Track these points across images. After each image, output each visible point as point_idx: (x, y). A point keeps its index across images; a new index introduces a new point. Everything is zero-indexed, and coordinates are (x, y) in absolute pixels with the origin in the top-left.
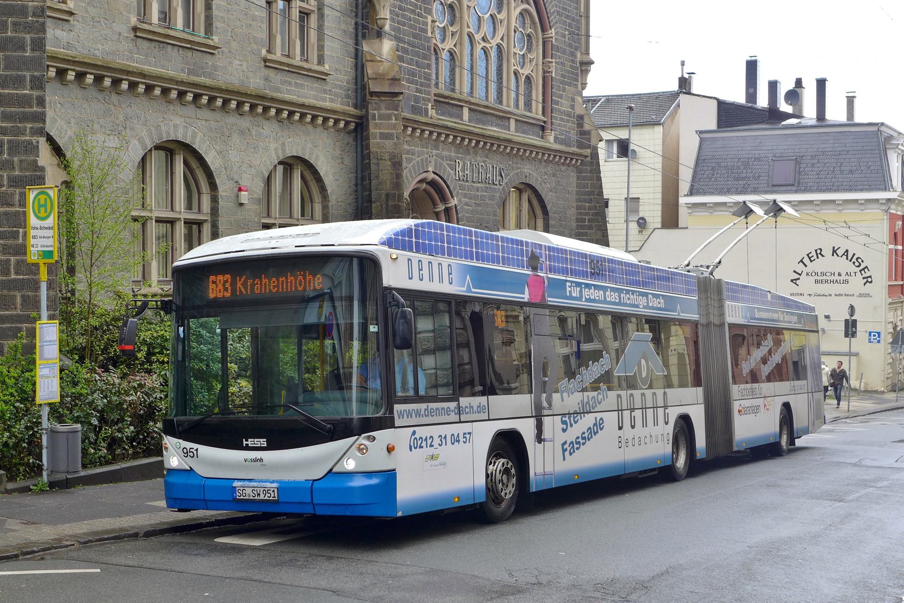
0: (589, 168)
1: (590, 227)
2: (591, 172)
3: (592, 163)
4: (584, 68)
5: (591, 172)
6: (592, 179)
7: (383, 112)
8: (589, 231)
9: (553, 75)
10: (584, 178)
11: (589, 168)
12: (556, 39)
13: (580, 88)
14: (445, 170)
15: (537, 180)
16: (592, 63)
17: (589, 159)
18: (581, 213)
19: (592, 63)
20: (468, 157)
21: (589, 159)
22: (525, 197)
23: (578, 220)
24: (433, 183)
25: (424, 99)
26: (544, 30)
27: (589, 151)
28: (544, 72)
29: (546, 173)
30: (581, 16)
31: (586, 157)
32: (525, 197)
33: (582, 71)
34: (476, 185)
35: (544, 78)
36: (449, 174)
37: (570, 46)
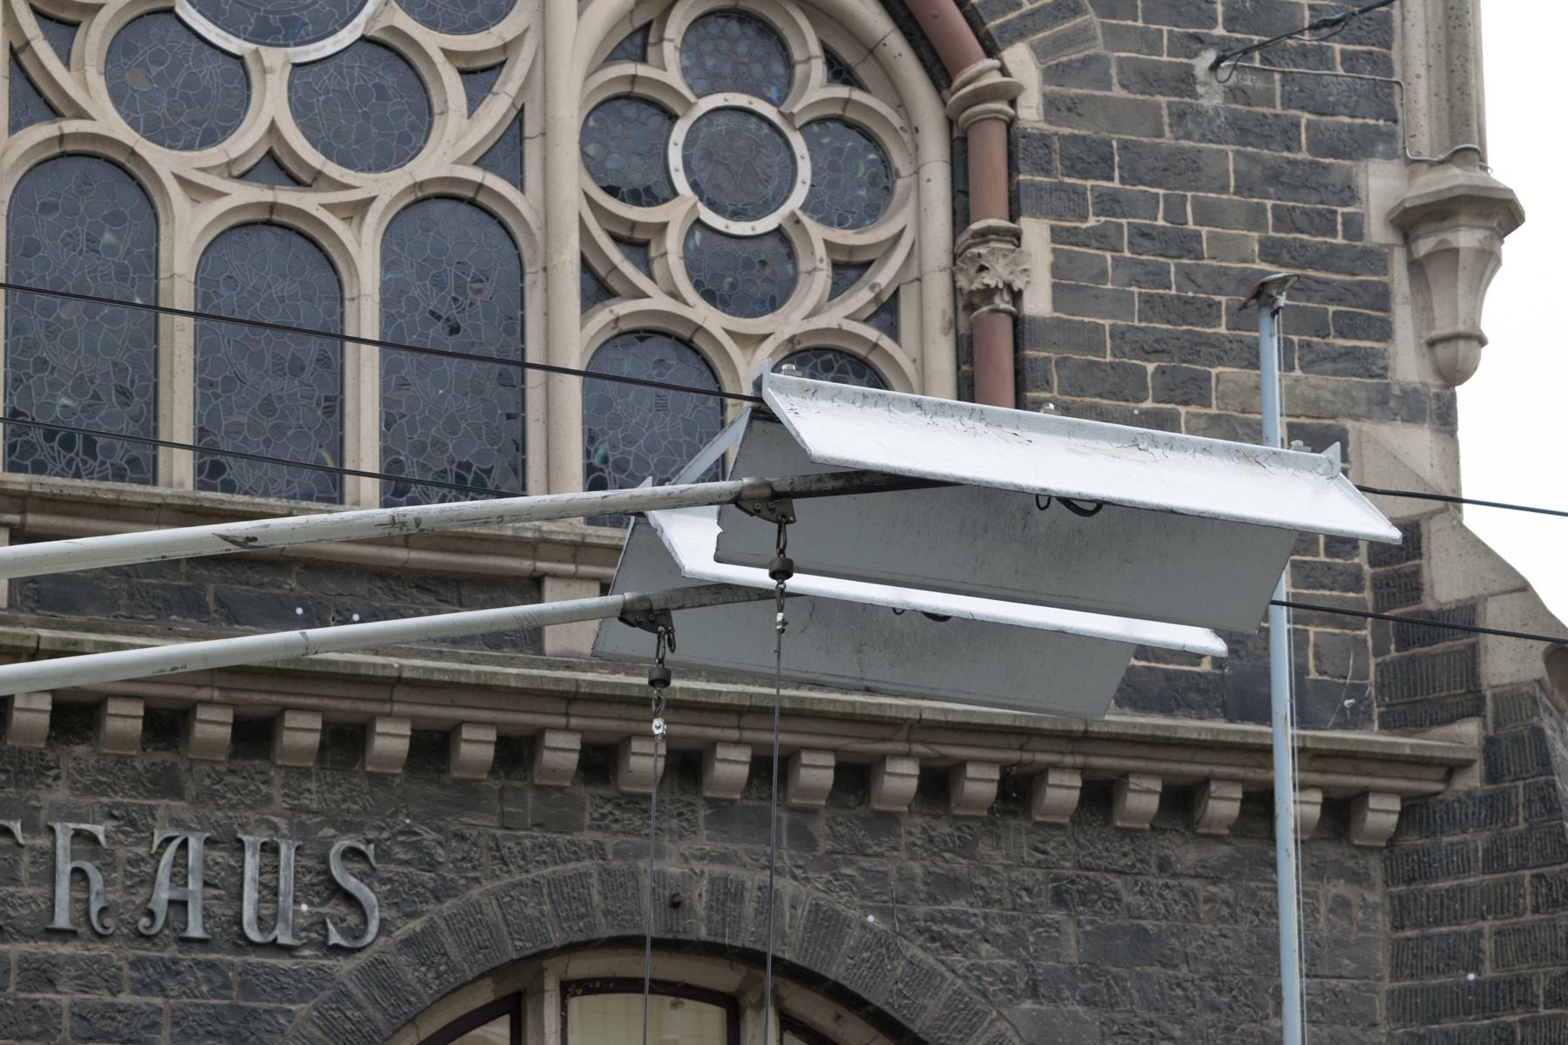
0: (1478, 840)
2: (1495, 858)
3: (1494, 807)
4: (1424, 246)
6: (1502, 904)
9: (1038, 303)
11: (1478, 840)
12: (1052, 105)
13: (1408, 364)
17: (1472, 781)
21: (1472, 781)
26: (940, 72)
27: (1470, 730)
28: (967, 302)
29: (953, 885)
31: (1452, 769)
33: (1416, 267)
37: (1242, 130)
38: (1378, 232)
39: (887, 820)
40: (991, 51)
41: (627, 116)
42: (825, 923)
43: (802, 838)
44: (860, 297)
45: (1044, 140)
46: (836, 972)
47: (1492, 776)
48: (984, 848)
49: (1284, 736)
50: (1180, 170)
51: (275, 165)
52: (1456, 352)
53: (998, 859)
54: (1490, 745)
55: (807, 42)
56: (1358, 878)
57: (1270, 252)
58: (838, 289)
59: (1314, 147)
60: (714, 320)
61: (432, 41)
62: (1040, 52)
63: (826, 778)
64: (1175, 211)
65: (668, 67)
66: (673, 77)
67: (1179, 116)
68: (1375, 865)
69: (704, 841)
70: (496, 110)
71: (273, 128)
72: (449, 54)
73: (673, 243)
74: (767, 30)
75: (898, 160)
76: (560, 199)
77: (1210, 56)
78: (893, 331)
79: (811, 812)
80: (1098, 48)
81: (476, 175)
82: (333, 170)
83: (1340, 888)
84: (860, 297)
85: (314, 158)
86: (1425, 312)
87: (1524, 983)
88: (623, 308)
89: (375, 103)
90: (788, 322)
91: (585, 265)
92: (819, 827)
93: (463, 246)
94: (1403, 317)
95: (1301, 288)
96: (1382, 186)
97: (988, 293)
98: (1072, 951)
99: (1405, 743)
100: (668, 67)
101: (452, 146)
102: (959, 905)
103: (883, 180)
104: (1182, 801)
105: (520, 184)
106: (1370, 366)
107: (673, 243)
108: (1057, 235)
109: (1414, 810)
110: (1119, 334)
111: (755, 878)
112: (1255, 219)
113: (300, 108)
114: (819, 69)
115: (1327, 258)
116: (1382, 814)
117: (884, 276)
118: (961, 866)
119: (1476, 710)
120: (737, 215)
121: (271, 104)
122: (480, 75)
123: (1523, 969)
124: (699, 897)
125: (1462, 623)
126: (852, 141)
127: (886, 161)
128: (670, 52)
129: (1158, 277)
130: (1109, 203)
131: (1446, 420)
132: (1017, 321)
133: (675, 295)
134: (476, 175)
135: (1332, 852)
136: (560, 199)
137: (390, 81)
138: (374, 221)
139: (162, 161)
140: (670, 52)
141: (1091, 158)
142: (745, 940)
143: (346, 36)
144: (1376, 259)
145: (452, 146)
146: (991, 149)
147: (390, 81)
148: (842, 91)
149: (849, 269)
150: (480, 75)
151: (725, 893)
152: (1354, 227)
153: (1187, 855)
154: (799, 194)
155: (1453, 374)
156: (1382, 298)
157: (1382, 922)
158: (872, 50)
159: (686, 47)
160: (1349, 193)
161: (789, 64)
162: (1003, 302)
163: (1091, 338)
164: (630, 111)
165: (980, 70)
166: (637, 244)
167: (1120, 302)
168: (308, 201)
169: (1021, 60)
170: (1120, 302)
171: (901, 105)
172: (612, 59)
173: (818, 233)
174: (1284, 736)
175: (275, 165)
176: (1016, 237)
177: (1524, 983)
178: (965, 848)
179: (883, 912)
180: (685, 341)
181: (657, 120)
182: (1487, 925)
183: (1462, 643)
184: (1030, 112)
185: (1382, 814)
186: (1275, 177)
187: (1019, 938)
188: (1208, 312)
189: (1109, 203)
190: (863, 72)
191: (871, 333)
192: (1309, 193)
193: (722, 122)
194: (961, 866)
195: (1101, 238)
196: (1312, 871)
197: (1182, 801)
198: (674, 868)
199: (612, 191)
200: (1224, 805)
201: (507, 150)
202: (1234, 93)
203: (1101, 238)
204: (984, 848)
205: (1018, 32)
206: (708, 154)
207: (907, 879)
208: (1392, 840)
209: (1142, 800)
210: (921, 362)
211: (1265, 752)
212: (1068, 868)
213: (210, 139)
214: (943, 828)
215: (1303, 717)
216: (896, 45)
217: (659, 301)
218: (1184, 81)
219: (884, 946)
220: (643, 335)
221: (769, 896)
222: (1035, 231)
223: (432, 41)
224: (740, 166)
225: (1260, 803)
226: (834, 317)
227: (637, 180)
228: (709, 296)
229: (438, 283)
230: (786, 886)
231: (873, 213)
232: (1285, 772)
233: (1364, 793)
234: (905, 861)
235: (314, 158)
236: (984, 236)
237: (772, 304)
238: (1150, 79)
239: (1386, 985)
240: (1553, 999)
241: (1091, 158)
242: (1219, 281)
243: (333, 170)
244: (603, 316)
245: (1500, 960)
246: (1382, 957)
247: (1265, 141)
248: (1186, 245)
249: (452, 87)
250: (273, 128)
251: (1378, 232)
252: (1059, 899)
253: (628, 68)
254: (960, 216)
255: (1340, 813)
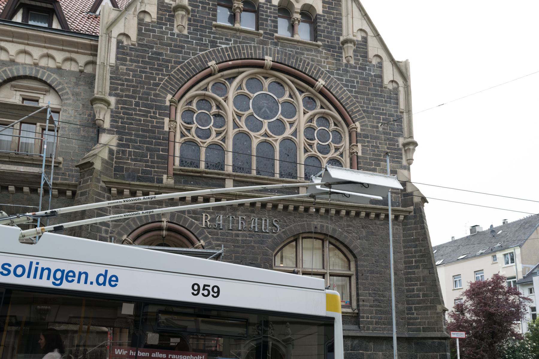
0: (413, 221)
1: (417, 267)
2: (415, 223)
3: (415, 217)
4: (406, 148)
5: (415, 223)
6: (416, 229)
7: (86, 178)
8: (416, 270)
9: (360, 154)
10: (410, 229)
11: (413, 221)
12: (361, 130)
13: (404, 163)
14: (186, 220)
15: (334, 230)
16: (415, 144)
17: (412, 214)
18: (408, 257)
19: (415, 144)
20: (222, 212)
21: (412, 214)
22: (327, 243)
23: (405, 262)
24: (169, 229)
25: (155, 172)
26: (348, 125)
27: (412, 208)
28: (351, 153)
29: (350, 226)
30: (402, 112)
31: (410, 212)
32: (327, 243)
33: (405, 151)
34: (234, 232)
35: (351, 160)
36: (192, 224)
37: (384, 133)
38: (401, 146)
39: (342, 217)
40: (354, 123)
41: (309, 130)
42: (334, 230)
43: (331, 220)
44: (338, 153)
45: (360, 134)
46: (335, 236)
47: (415, 213)
48: (354, 221)
49: (390, 208)
50: (377, 138)
51: (266, 135)
52: (410, 161)
53: (355, 223)
54: (414, 209)
55: (331, 121)
56: (399, 225)
57: (388, 148)
58: (335, 152)
59: (393, 135)
60: (320, 155)
61: (285, 120)
62: (360, 123)
63: (334, 212)
64: (376, 143)
65: (314, 124)
66: (315, 125)
67: (377, 131)
68: (401, 224)
69: (319, 220)
70: (293, 128)
71: (266, 130)
72: (288, 121)
73: (315, 145)
74: (327, 119)
75: (343, 136)
76: (301, 140)
77: (380, 124)
78: (342, 157)
79: (332, 216)
80: (367, 123)
81: (291, 136)
82: (273, 135)
83: (397, 227)
84: (338, 153)
85: (271, 134)
86: (406, 156)
87: (419, 238)
88: (309, 153)
89: (278, 127)
90: (329, 156)
91: (304, 148)
92: (333, 218)
93: (289, 145)
94: (404, 157)
95: (391, 153)
96: (401, 141)
97: (354, 153)
98: (364, 234)
99: (404, 209)
100: (314, 124)
101: (288, 133)
102: (350, 228)
103: (341, 138)
104: (377, 216)
105: (296, 138)
106: (400, 163)
107: (315, 145)
108: (362, 146)
109: (405, 217)
110: (369, 158)
111: (325, 225)
112: (386, 144)
113: (269, 128)
114: (333, 124)
115: (394, 149)
116: (402, 218)
117: (341, 150)
118: (351, 223)
119: (413, 205)
120: (323, 142)
121: (265, 127)
122: (291, 124)
123: (418, 237)
124: (319, 227)
125: (411, 194)
126: (337, 133)
127: (341, 136)
128: (315, 122)
129: (374, 151)
130: (368, 142)
131: (409, 169)
132: (357, 156)
133: (315, 152)
134: (291, 136)
135: (396, 222)
136: (301, 140)
137: (280, 124)
138: (278, 142)
139: (252, 134)
140: (315, 122)
141: (366, 136)
142: (324, 232)
143: (275, 119)
144: (400, 150)
145: (288, 133)
146: (354, 135)
147: (280, 124)
148: (336, 127)
149: (337, 149)
150: (291, 124)
151: (322, 226)
152: (398, 145)
153: (378, 222)
154: (331, 140)
155: (410, 164)
156: (401, 154)
157: (402, 231)
158: (339, 122)
159: (317, 121)
160: (397, 141)
161: (329, 124)
162: (355, 154)
163: (366, 159)
164: (310, 129)
165: (353, 125)
166: (311, 145)
167: (370, 154)
168: (270, 139)
169: (358, 124)
170: (370, 154)
171: (343, 129)
172: (308, 122)
173: (333, 145)
174: (390, 208)
175: (266, 135)
176: (357, 146)
177: (419, 238)
178: (351, 221)
179: (341, 229)
180: (317, 158)
181: (313, 130)
182: (414, 231)
183: (411, 197)
184: (359, 130)
185: (402, 218)
186: (388, 139)
187: (358, 232)
188: (380, 156)
189: (368, 142)
190: (338, 125)
191: (339, 157)
192: (393, 141)
193: (321, 131)
194: (351, 223)
195: (368, 146)
196: (393, 225)
197: (377, 216)
198: (315, 223)
199: (308, 139)
200: (383, 216)
201: (295, 133)
202: (383, 129)
203: (368, 146)
204: (354, 221)
205: (357, 120)
206: (320, 135)
207: (344, 225)
208: (403, 221)
209: (373, 215)
210: (346, 161)
211: (388, 210)
212: (364, 224)
213: (258, 131)
214: (349, 219)
215: (392, 206)
216: (342, 122)
217: (313, 153)
218: (377, 127)
219: (341, 233)
220: (312, 157)
221: (327, 227)
222: (359, 145)
223: (285, 120)
224: (323, 136)
225: (387, 216)
226: (335, 155)
227: (311, 137)
228: (320, 152)
229: (286, 150)
230: (330, 226)
231: (340, 142)
232: (390, 212)
233: (399, 215)
234: (344, 223)
235: (271, 134)
236: (353, 145)
237: (327, 153)
238: (373, 127)
239: (402, 239)
240: (422, 241)
241: (366, 136)
242: (382, 152)
243: (273, 135)
244: (307, 154)
245: (416, 236)
246: (402, 235)
247: (387, 135)
248: (378, 147)
249: (288, 125)
250: (266, 130)
251: (401, 146)
252: (363, 228)
253: (310, 124)
254: (350, 143)
255: (396, 217)
